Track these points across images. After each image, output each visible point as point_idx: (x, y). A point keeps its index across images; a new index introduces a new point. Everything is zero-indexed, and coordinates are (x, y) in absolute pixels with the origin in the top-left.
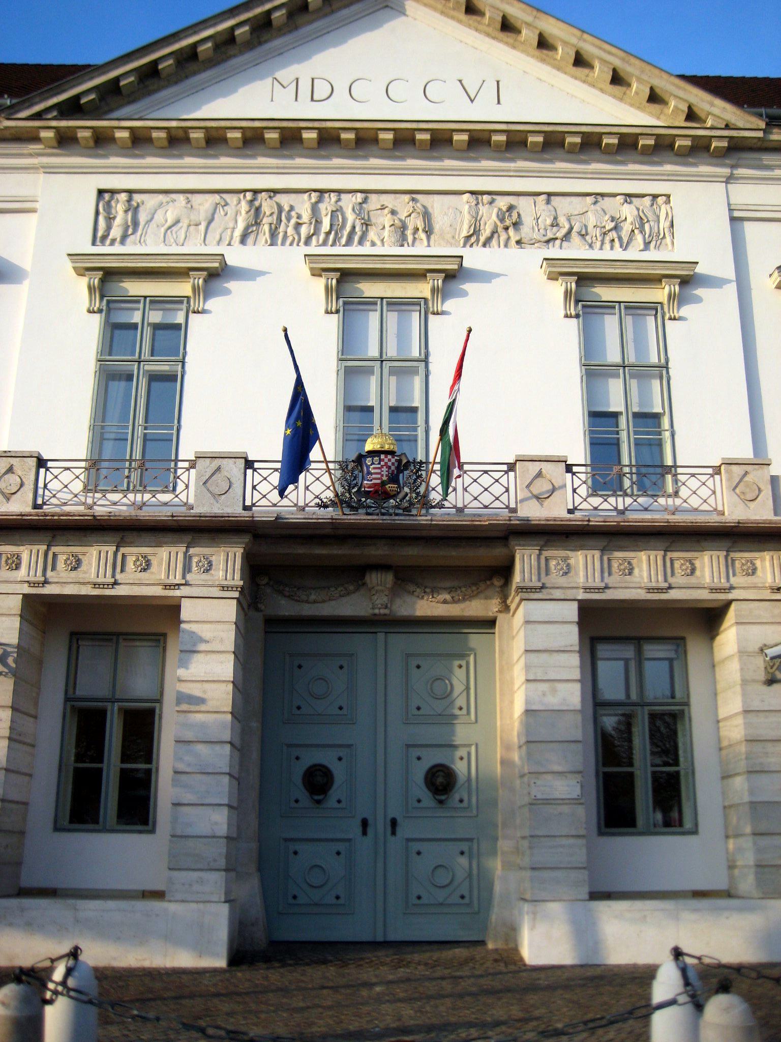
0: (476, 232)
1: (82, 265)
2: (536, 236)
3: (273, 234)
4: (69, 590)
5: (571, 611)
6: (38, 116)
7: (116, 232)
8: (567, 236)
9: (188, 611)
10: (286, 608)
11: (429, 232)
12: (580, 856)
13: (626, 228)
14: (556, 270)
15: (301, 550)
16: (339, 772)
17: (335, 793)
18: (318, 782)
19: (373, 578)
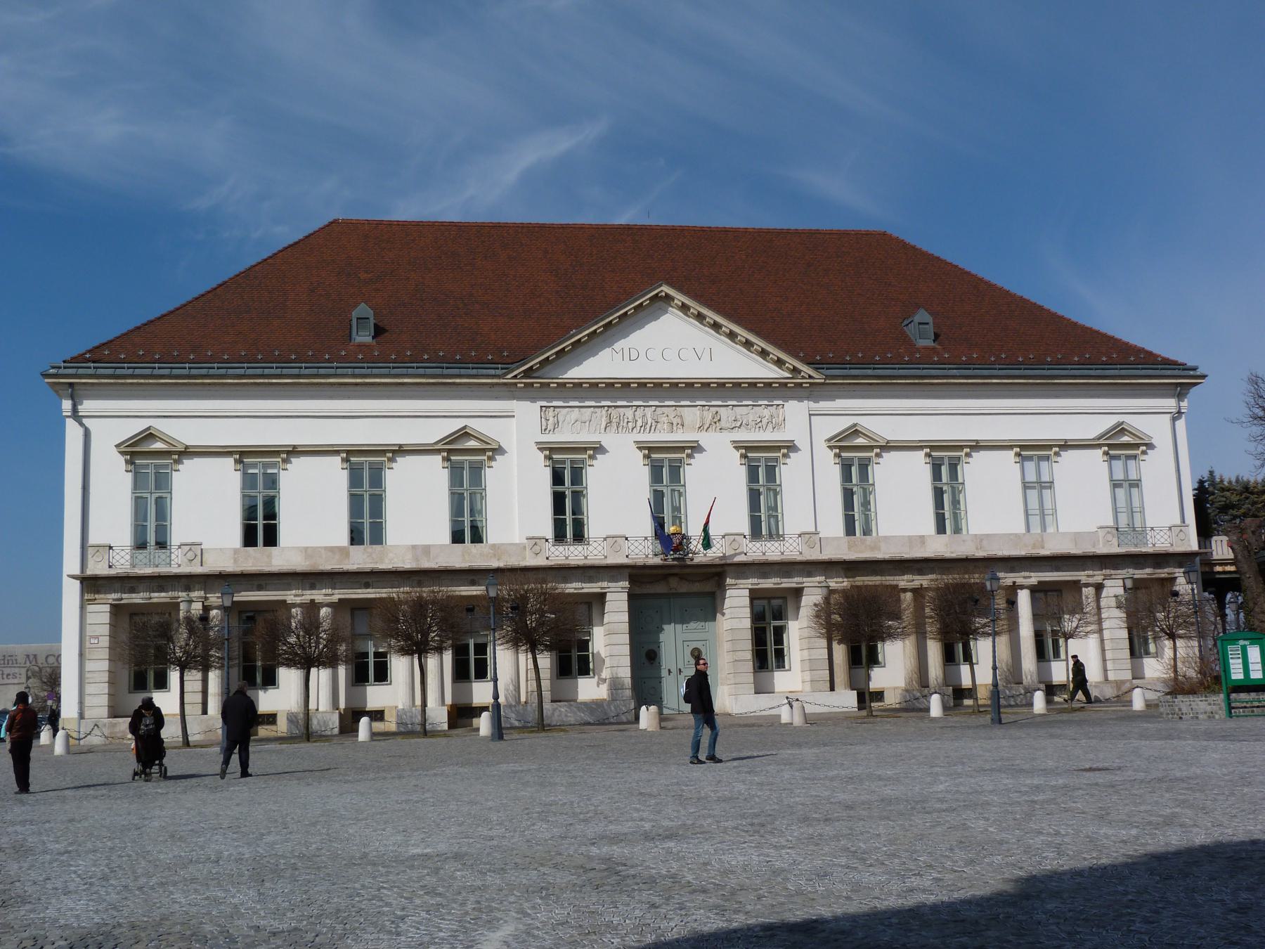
2: (728, 425)
6: (515, 377)
9: (609, 597)
10: (638, 591)
13: (765, 421)
14: (738, 445)
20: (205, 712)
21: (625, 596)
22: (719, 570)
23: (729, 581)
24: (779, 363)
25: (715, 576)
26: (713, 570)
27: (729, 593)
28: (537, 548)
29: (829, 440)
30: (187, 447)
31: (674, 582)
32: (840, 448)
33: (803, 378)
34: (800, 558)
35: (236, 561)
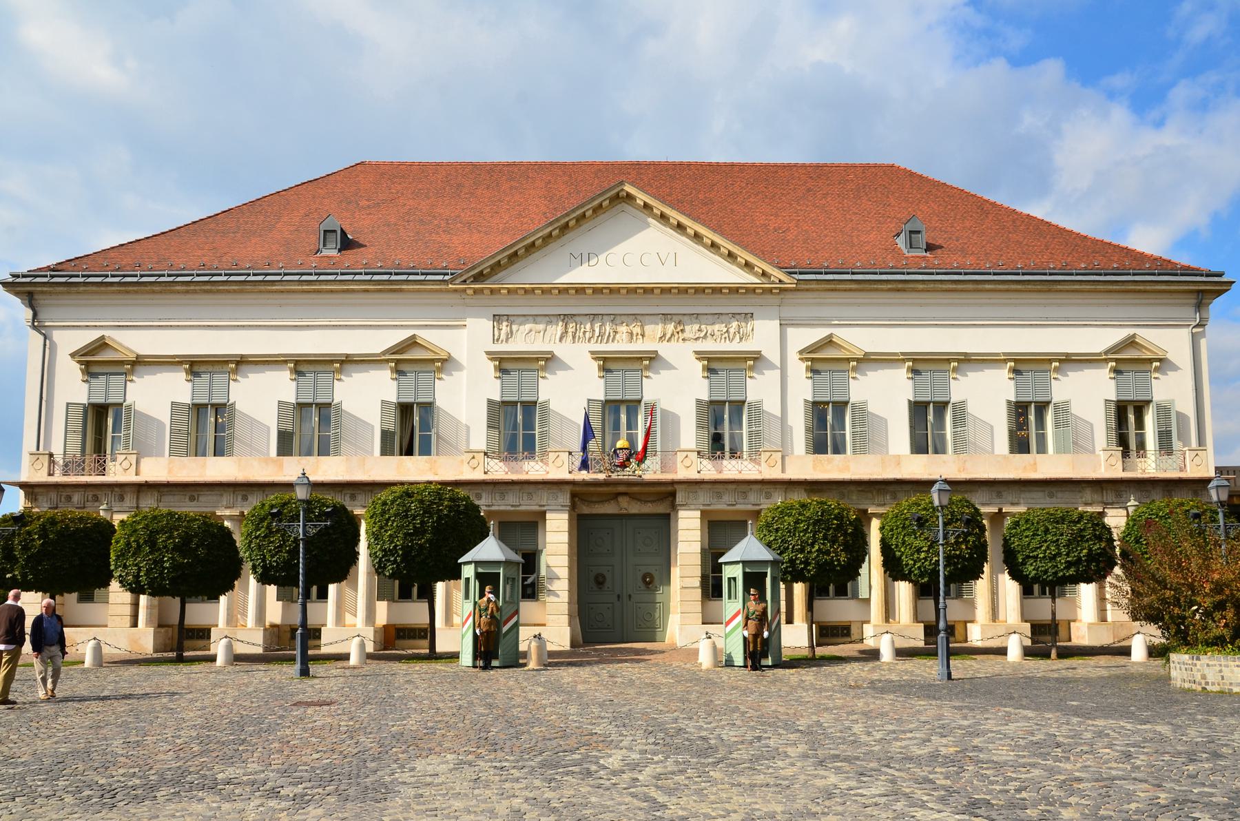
0: (664, 335)
1: (492, 355)
2: (691, 336)
3: (574, 337)
4: (502, 508)
5: (698, 514)
7: (503, 336)
8: (705, 337)
9: (548, 516)
10: (586, 510)
11: (643, 336)
12: (699, 609)
14: (700, 355)
15: (592, 489)
16: (609, 577)
17: (608, 584)
18: (600, 581)
19: (620, 499)
20: (135, 625)
21: (566, 516)
22: (670, 488)
23: (680, 498)
24: (748, 266)
25: (667, 494)
26: (663, 489)
27: (682, 514)
28: (474, 462)
29: (801, 352)
30: (138, 356)
31: (624, 501)
32: (812, 360)
33: (773, 283)
34: (759, 477)
35: (170, 471)
